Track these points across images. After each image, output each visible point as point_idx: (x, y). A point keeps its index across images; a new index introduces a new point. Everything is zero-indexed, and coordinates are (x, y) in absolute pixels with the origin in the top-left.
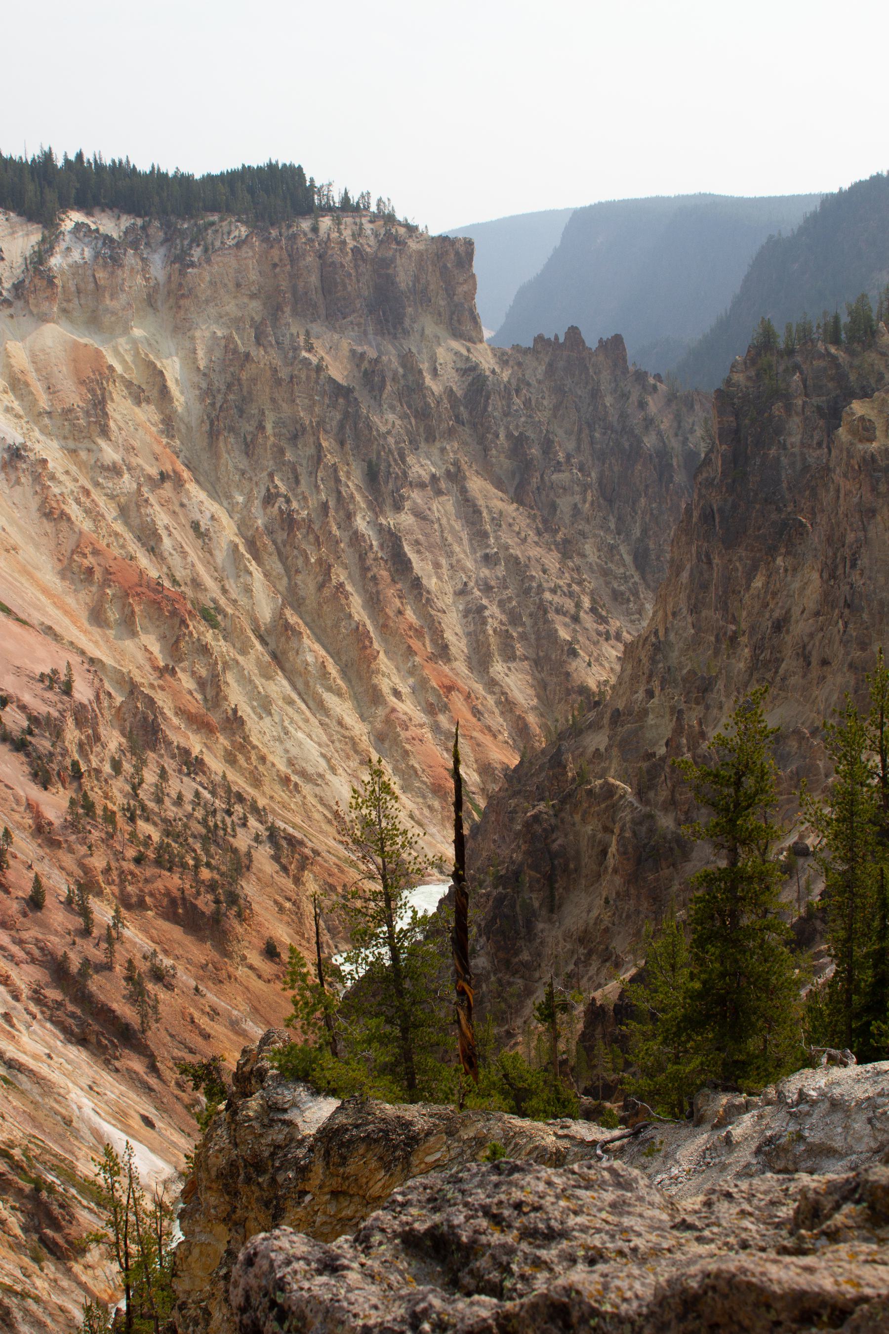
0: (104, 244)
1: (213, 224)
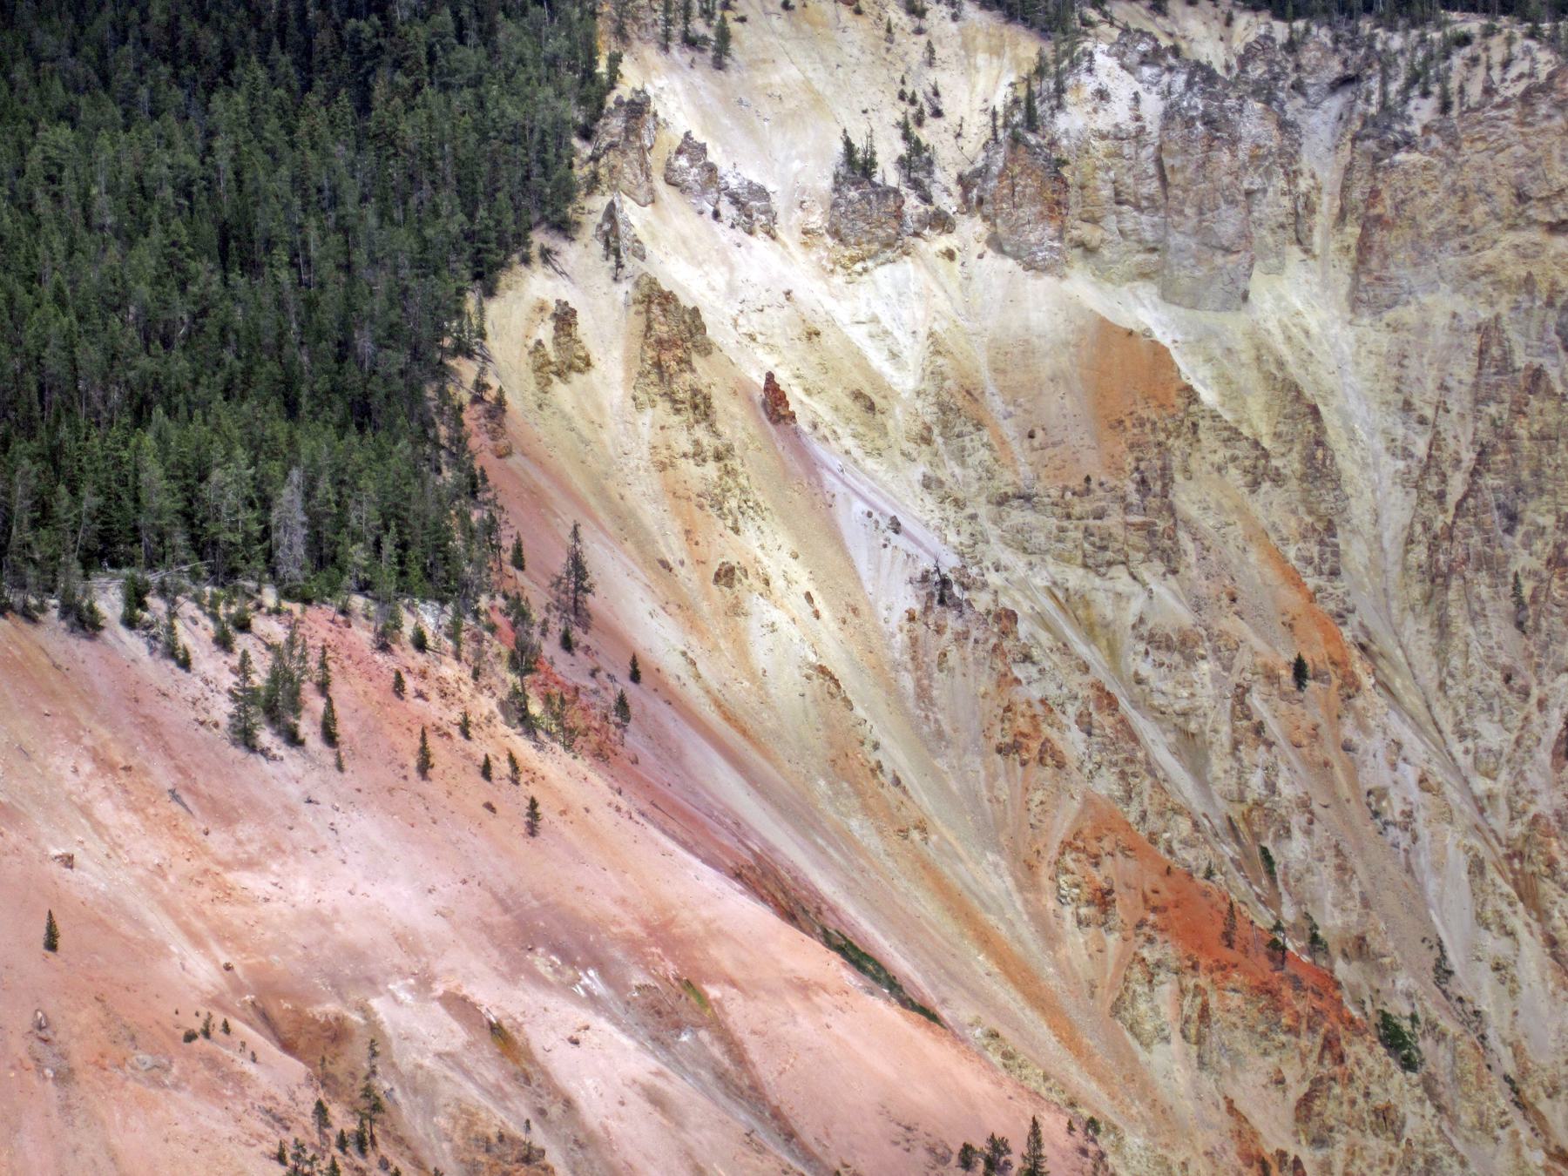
0: (1189, 85)
1: (1465, 40)
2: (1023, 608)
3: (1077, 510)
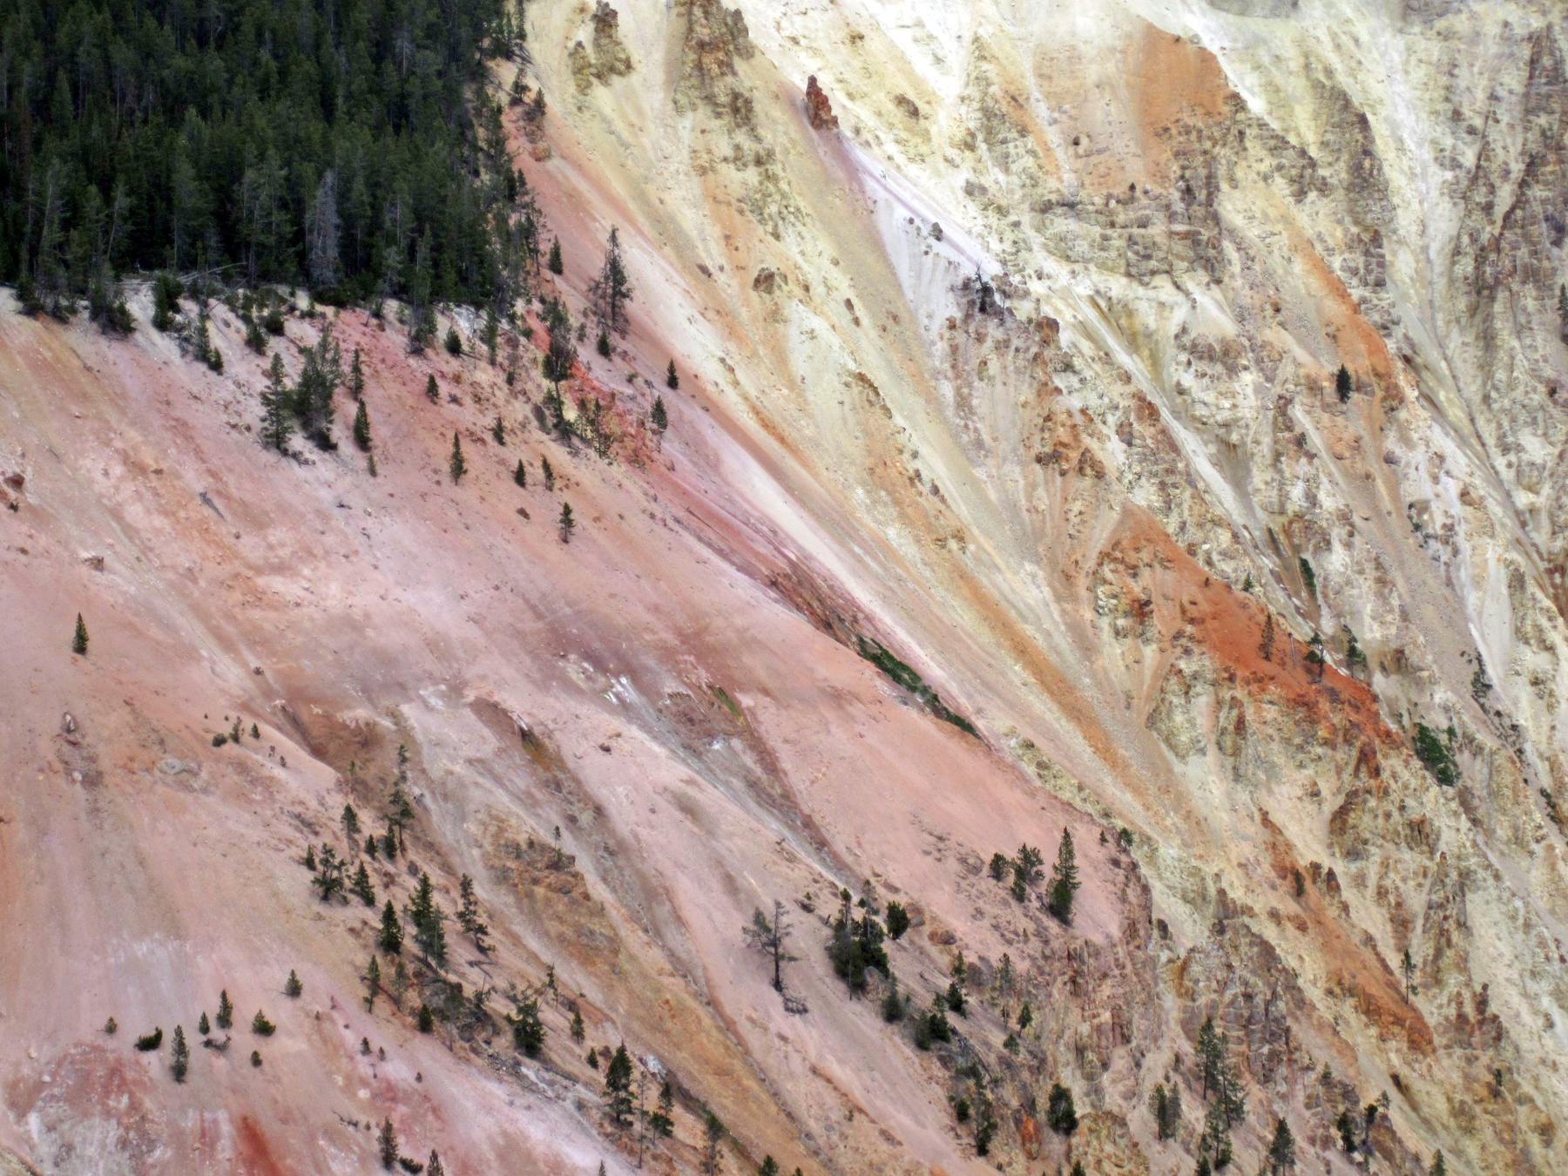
2: (1065, 317)
3: (1121, 218)
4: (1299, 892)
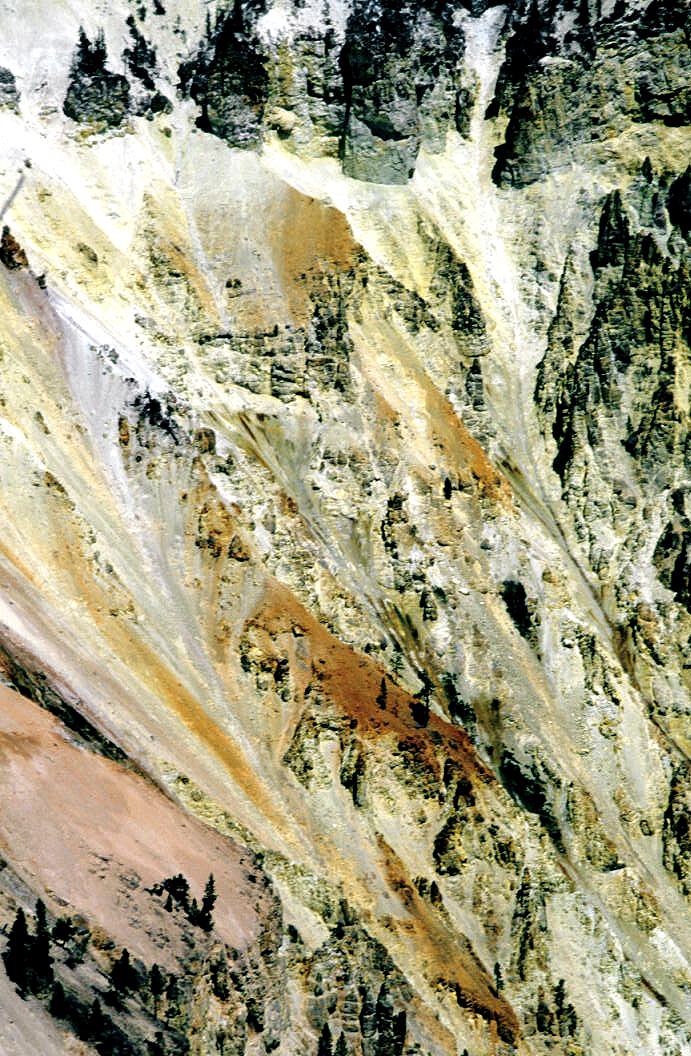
4: (408, 902)
